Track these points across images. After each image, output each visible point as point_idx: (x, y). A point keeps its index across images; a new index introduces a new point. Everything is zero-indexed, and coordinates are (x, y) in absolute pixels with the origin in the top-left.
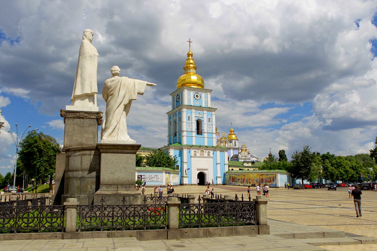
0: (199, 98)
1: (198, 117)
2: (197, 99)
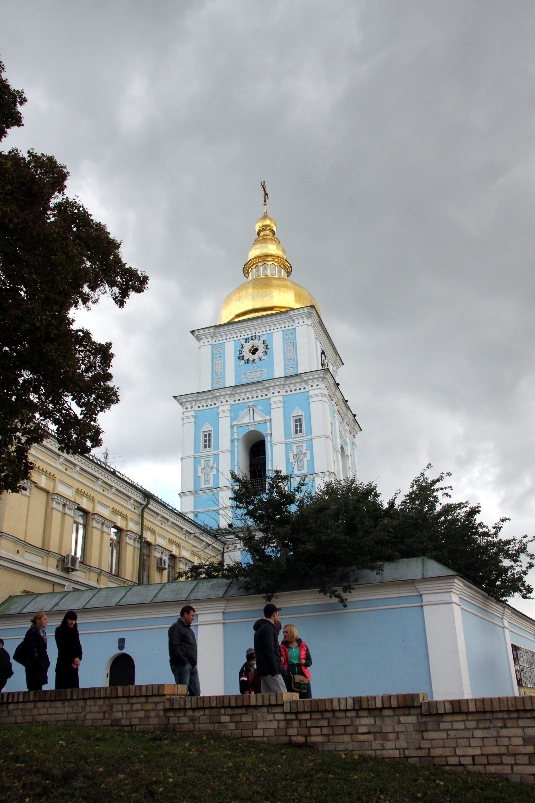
0: (259, 353)
1: (246, 425)
2: (254, 361)
